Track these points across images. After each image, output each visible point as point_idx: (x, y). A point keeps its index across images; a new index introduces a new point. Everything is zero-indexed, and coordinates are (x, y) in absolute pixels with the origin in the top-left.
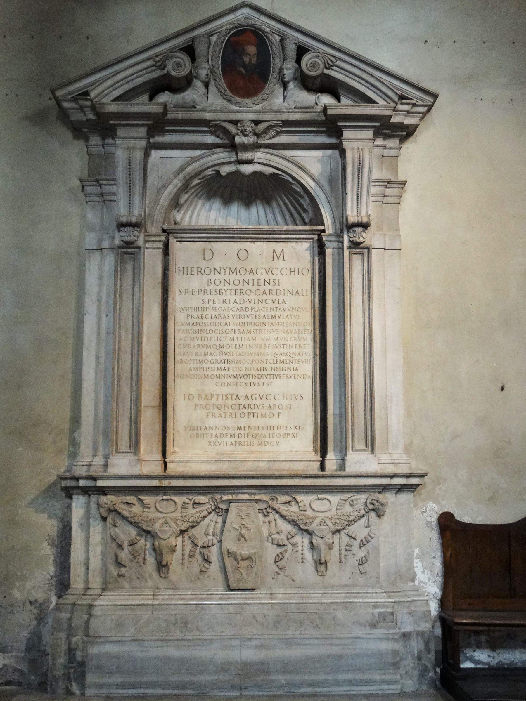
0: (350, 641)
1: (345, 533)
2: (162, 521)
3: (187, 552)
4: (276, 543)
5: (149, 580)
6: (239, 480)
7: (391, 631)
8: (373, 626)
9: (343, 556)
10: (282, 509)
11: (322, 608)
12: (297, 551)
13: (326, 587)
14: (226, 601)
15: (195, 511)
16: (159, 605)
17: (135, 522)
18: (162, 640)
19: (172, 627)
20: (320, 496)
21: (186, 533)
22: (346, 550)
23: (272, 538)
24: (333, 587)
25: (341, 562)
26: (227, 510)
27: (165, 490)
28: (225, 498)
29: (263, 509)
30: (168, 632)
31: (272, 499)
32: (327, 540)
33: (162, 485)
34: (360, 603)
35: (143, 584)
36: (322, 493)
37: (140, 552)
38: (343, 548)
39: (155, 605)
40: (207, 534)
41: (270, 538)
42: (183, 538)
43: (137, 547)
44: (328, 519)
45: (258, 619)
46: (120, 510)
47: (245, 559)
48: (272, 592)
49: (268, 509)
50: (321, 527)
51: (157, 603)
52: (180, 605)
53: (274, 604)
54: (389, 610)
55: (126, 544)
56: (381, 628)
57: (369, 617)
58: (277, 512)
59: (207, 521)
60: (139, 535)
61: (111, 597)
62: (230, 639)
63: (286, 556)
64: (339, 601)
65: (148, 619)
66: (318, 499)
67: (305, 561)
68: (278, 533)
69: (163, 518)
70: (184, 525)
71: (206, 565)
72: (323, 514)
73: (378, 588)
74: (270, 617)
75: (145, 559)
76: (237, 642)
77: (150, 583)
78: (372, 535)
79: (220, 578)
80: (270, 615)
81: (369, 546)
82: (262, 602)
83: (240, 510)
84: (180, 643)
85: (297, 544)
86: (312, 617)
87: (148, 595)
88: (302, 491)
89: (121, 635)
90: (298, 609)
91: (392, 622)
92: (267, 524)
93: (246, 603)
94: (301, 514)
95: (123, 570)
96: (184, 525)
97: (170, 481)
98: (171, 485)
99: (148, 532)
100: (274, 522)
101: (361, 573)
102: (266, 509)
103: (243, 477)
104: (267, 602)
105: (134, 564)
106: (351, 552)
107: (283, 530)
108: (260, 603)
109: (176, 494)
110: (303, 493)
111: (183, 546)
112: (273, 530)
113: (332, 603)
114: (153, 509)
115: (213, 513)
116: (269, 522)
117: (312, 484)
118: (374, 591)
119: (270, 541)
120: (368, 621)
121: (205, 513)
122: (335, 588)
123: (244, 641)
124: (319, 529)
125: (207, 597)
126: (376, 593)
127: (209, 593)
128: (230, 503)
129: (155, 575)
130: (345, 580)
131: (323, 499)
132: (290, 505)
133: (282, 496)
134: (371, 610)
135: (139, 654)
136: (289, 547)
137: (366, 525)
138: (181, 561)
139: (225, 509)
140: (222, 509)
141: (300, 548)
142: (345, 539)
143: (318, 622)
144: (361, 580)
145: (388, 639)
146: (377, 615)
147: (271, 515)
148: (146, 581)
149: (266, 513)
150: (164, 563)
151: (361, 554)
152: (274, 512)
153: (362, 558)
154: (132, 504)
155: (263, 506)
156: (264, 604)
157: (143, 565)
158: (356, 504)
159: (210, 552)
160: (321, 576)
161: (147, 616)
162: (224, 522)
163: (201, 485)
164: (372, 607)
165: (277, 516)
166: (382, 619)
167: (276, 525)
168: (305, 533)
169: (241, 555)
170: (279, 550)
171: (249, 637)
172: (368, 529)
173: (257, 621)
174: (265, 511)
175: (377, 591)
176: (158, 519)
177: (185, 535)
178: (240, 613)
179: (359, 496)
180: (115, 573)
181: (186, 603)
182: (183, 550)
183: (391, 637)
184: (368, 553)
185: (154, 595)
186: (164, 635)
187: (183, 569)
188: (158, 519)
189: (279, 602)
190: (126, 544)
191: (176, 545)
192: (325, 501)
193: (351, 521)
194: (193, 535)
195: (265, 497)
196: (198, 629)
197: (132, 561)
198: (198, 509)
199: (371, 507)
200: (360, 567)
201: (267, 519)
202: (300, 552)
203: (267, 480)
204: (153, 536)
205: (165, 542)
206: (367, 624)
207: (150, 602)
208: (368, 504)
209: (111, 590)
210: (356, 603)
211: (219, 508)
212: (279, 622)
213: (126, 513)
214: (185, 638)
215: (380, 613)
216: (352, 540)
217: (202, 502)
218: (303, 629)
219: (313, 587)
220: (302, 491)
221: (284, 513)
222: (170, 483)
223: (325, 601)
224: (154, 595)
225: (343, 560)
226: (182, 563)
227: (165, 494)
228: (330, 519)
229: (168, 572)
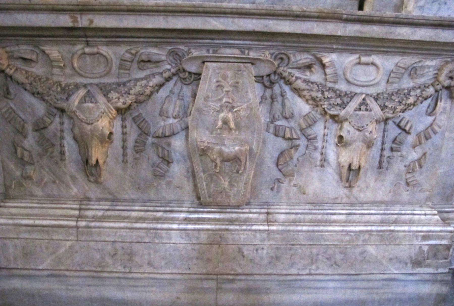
0: (380, 284)
1: (395, 123)
2: (82, 92)
3: (131, 143)
4: (281, 134)
5: (72, 186)
6: (222, 20)
7: (440, 271)
8: (417, 263)
9: (385, 159)
10: (297, 78)
11: (347, 238)
12: (316, 149)
13: (352, 205)
14: (195, 224)
15: (142, 74)
16: (87, 227)
17: (38, 93)
18: (93, 277)
19: (110, 261)
20: (364, 59)
21: (128, 113)
22: (392, 150)
23: (276, 127)
24: (362, 204)
25: (380, 167)
26: (198, 76)
27: (86, 37)
28: (195, 53)
29: (262, 77)
30: (104, 267)
31: (282, 59)
32: (367, 134)
33: (76, 25)
34: (404, 231)
35: (64, 191)
36: (368, 53)
37: (54, 141)
38: (387, 146)
39: (81, 227)
40: (163, 114)
41: (272, 126)
42: (123, 120)
43: (49, 133)
44: (372, 99)
45: (246, 253)
46: (10, 72)
47: (228, 160)
48: (270, 211)
49: (272, 77)
50: (361, 113)
51: (83, 224)
52: (121, 228)
53: (273, 231)
54: (444, 242)
55: (29, 128)
56: (428, 266)
57: (413, 252)
58: (288, 83)
59: (163, 93)
60: (50, 114)
61: (13, 211)
62: (202, 280)
63: (296, 155)
64: (374, 228)
65: (71, 247)
66: (359, 63)
67: (325, 164)
68: (286, 118)
69: (85, 86)
70: (122, 100)
71: (164, 167)
72: (364, 90)
73: (428, 206)
74: (265, 251)
75: (62, 153)
76: (212, 284)
77: (74, 190)
78: (436, 128)
79: (188, 187)
80: (265, 247)
81: (428, 146)
82: (254, 228)
83: (225, 78)
84: (124, 282)
85: (315, 138)
86: (330, 252)
87: (72, 209)
88: (335, 47)
89: (32, 267)
90: (311, 240)
91: (446, 259)
92: (269, 100)
93: (227, 230)
94: (330, 88)
95: (30, 170)
96: (122, 100)
97: (90, 16)
98: (93, 25)
99: (62, 111)
100: (279, 99)
101: (408, 184)
102: (269, 75)
103: (232, 13)
104: (261, 228)
105: (45, 161)
106: (399, 154)
107: (295, 113)
108: (250, 230)
109: (107, 44)
110: (333, 51)
111: (124, 134)
112: (277, 114)
113: (361, 232)
114: (68, 71)
115: (175, 78)
116: (272, 99)
117: (357, 35)
118: (423, 212)
119: (271, 130)
120: (411, 257)
121: (157, 80)
122: (366, 206)
123: (220, 283)
124: (357, 115)
125: (165, 215)
126: (425, 215)
127: (168, 209)
128: (204, 62)
129: (81, 177)
130: (381, 195)
131: (367, 64)
132: (311, 72)
133: (297, 54)
134: (417, 243)
135: (64, 294)
136: (303, 142)
137: (429, 111)
138: (121, 159)
139: (195, 74)
140: (190, 73)
141: (319, 144)
142: (393, 132)
143: (338, 257)
144: (405, 195)
145: (434, 281)
146: (426, 249)
147: (277, 88)
148: (68, 186)
149: (267, 84)
150: (93, 161)
151: (414, 155)
152: (282, 82)
153: (414, 162)
154: (31, 60)
155: (265, 70)
156: (256, 231)
157: (60, 162)
158: (423, 76)
159: (169, 145)
160: (347, 187)
161: (68, 244)
162: (194, 96)
163: (150, 26)
164: (420, 238)
165: (287, 88)
166: (431, 254)
167: (283, 105)
168: (331, 120)
169: (220, 153)
170: (284, 145)
171: (231, 277)
172: (430, 119)
173: (244, 256)
174: (266, 79)
175: (427, 212)
176: (77, 87)
177: (127, 115)
178: (219, 245)
179: (428, 63)
180: (18, 173)
181: (129, 225)
182: (124, 141)
183: (439, 278)
184: (425, 154)
185: (80, 209)
186: (99, 269)
187: (124, 170)
188: (77, 87)
189: (280, 228)
190: (29, 128)
191: (111, 133)
192: (371, 69)
193: (409, 105)
194: (140, 115)
195: (267, 55)
196: (150, 264)
197: (41, 156)
198: (148, 72)
199: (447, 83)
200: (409, 176)
201: (269, 92)
202: (319, 150)
203: (275, 22)
204: (71, 118)
205: (89, 127)
206: (409, 261)
207: (73, 223)
208: (442, 78)
209: (14, 198)
210: (398, 231)
211: (184, 71)
212: (277, 258)
213: (20, 77)
214: (130, 275)
215: (430, 245)
216: (404, 133)
217: (154, 58)
218: (314, 267)
219: (335, 202)
220: (335, 47)
221: (300, 84)
222: (91, 21)
223: (352, 228)
224: (80, 209)
225: (385, 164)
226: (123, 161)
227: (88, 44)
228: (376, 99)
229: (100, 176)
